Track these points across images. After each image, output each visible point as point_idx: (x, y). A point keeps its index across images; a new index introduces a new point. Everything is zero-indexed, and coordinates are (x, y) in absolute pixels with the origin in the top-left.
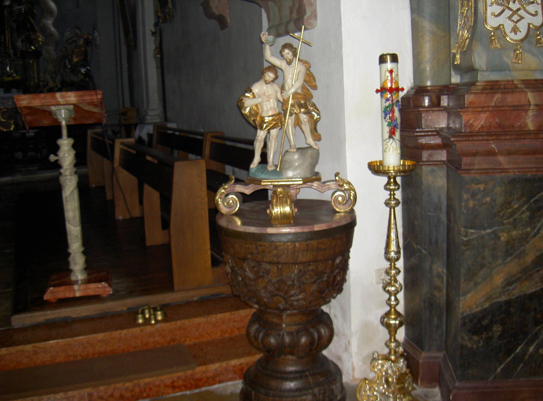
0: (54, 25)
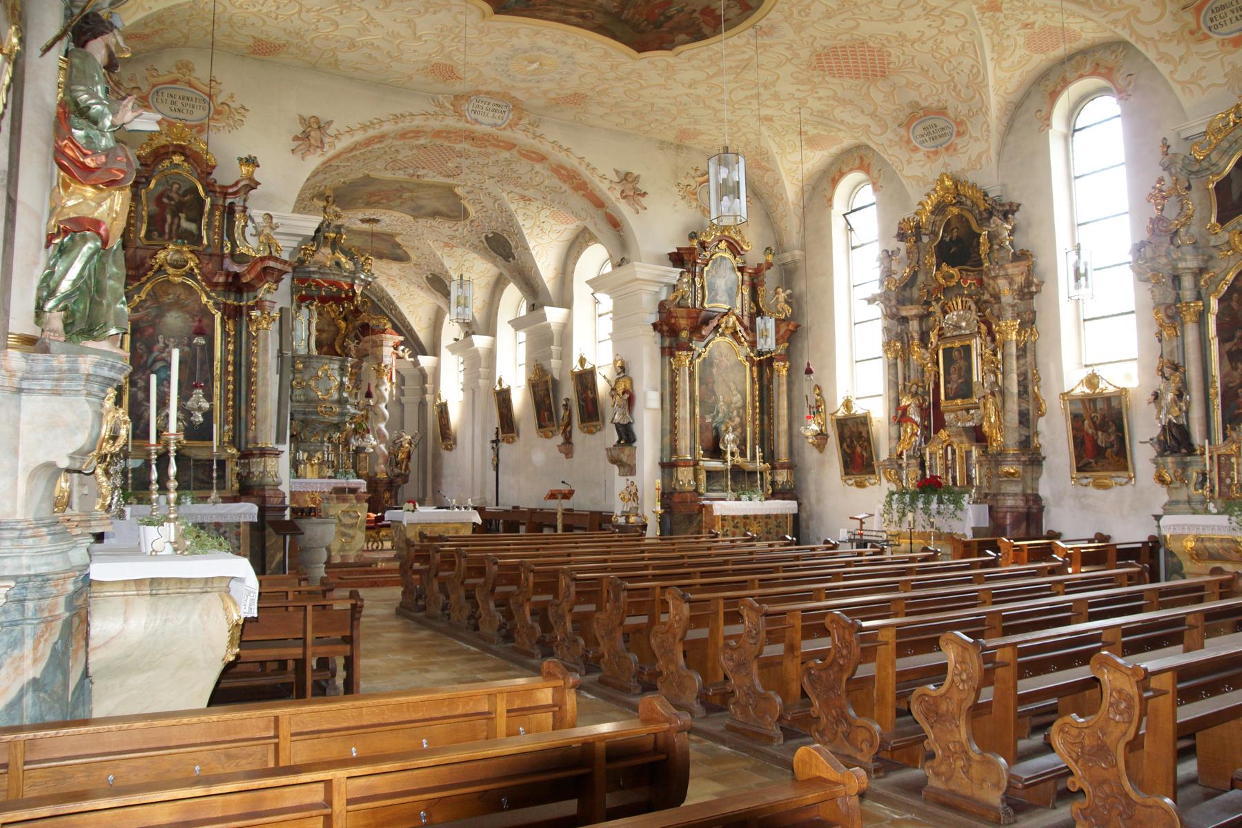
0: (386, 427)
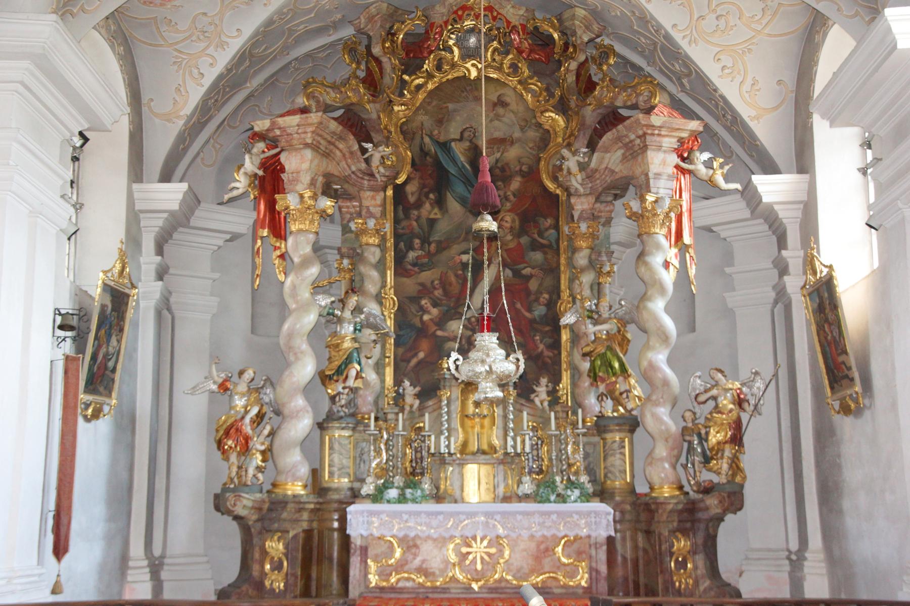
0: (670, 361)
